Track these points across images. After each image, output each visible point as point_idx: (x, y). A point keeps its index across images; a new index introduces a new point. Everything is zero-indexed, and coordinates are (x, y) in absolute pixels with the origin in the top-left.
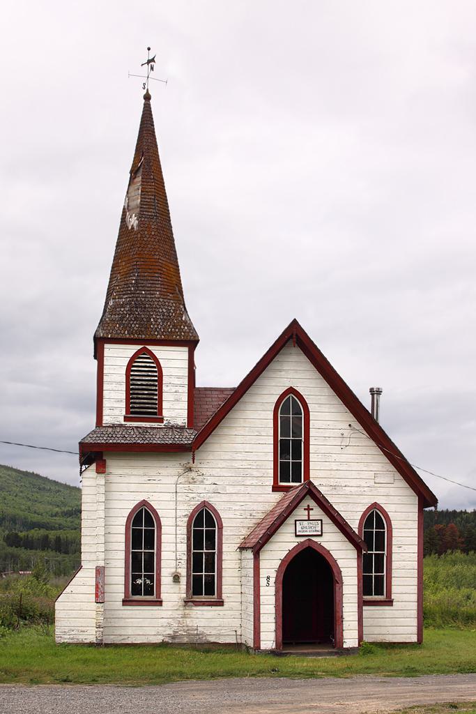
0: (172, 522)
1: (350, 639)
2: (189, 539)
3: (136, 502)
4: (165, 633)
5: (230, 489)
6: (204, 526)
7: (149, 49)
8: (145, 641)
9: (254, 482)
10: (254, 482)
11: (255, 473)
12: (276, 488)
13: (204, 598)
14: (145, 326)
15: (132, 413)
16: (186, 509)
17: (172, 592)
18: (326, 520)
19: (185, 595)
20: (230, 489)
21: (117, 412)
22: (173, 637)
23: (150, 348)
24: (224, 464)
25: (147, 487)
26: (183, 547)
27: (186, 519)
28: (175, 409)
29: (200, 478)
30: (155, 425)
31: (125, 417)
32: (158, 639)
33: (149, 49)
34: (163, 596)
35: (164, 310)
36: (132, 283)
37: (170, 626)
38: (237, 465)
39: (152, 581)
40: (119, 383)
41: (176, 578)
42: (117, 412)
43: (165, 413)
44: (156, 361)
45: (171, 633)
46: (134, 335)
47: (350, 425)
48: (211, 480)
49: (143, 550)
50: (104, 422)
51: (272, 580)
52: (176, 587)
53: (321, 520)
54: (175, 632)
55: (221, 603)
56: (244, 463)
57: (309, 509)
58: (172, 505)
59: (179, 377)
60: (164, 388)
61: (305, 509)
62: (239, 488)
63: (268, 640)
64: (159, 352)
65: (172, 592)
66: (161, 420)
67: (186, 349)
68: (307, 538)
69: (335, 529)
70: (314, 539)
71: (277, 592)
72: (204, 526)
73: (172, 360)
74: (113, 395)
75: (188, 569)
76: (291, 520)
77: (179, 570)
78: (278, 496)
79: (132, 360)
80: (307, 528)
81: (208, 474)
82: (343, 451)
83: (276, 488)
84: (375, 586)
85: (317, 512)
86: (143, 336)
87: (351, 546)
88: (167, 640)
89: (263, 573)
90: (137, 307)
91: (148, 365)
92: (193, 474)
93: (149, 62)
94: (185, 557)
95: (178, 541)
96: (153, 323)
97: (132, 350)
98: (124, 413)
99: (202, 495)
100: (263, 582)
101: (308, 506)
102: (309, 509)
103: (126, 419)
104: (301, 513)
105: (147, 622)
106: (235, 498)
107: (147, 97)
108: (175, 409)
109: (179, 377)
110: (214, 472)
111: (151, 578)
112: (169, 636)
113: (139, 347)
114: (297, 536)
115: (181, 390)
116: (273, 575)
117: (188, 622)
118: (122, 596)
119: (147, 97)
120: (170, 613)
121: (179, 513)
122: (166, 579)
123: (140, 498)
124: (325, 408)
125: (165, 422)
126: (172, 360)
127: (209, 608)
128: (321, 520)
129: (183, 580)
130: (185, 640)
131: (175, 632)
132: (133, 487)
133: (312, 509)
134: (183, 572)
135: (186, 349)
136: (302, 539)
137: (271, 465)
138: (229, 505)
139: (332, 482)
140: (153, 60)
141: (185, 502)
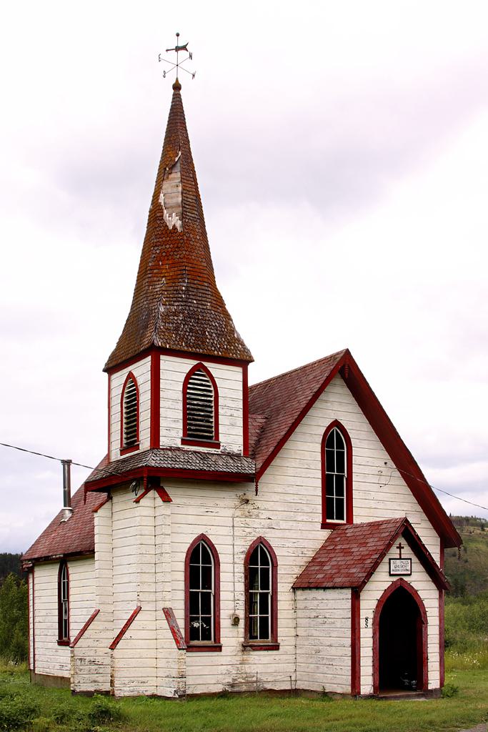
0: (230, 559)
1: (433, 682)
3: (195, 536)
4: (224, 682)
5: (283, 525)
6: (259, 562)
7: (178, 35)
8: (206, 691)
9: (305, 518)
11: (306, 509)
12: (325, 526)
13: (259, 642)
14: (201, 338)
16: (243, 546)
17: (231, 636)
19: (243, 640)
20: (283, 525)
21: (173, 433)
22: (232, 686)
23: (206, 364)
24: (276, 497)
25: (205, 520)
28: (231, 435)
29: (256, 512)
30: (213, 451)
31: (182, 440)
32: (218, 688)
33: (178, 35)
34: (223, 641)
35: (217, 325)
36: (182, 290)
37: (229, 673)
38: (289, 498)
40: (175, 400)
41: (236, 621)
42: (173, 433)
43: (222, 439)
45: (231, 681)
46: (191, 348)
47: (386, 463)
48: (265, 514)
49: (200, 590)
51: (370, 621)
52: (235, 629)
53: (411, 559)
54: (234, 680)
55: (276, 647)
56: (295, 497)
57: (400, 547)
59: (233, 400)
61: (397, 548)
62: (291, 523)
63: (367, 686)
64: (216, 369)
65: (231, 636)
66: (217, 446)
67: (240, 369)
68: (398, 578)
71: (374, 633)
72: (259, 562)
73: (227, 379)
76: (386, 560)
77: (237, 612)
78: (326, 534)
79: (188, 377)
80: (399, 567)
81: (263, 508)
82: (381, 489)
83: (325, 526)
85: (407, 551)
86: (201, 351)
90: (190, 318)
91: (204, 383)
92: (249, 507)
93: (178, 49)
95: (236, 580)
96: (209, 337)
97: (188, 364)
98: (181, 434)
99: (257, 530)
100: (363, 622)
101: (400, 544)
102: (400, 547)
103: (184, 442)
104: (394, 552)
105: (207, 670)
106: (287, 534)
107: (177, 87)
108: (231, 435)
109: (233, 400)
110: (267, 505)
111: (207, 621)
114: (391, 575)
115: (236, 413)
116: (371, 616)
117: (247, 669)
119: (177, 87)
120: (229, 658)
121: (238, 549)
122: (225, 623)
124: (365, 444)
125: (221, 448)
126: (227, 379)
127: (265, 652)
128: (411, 559)
129: (242, 623)
130: (244, 688)
131: (234, 680)
132: (191, 519)
133: (403, 548)
135: (240, 369)
136: (395, 579)
140: (184, 48)
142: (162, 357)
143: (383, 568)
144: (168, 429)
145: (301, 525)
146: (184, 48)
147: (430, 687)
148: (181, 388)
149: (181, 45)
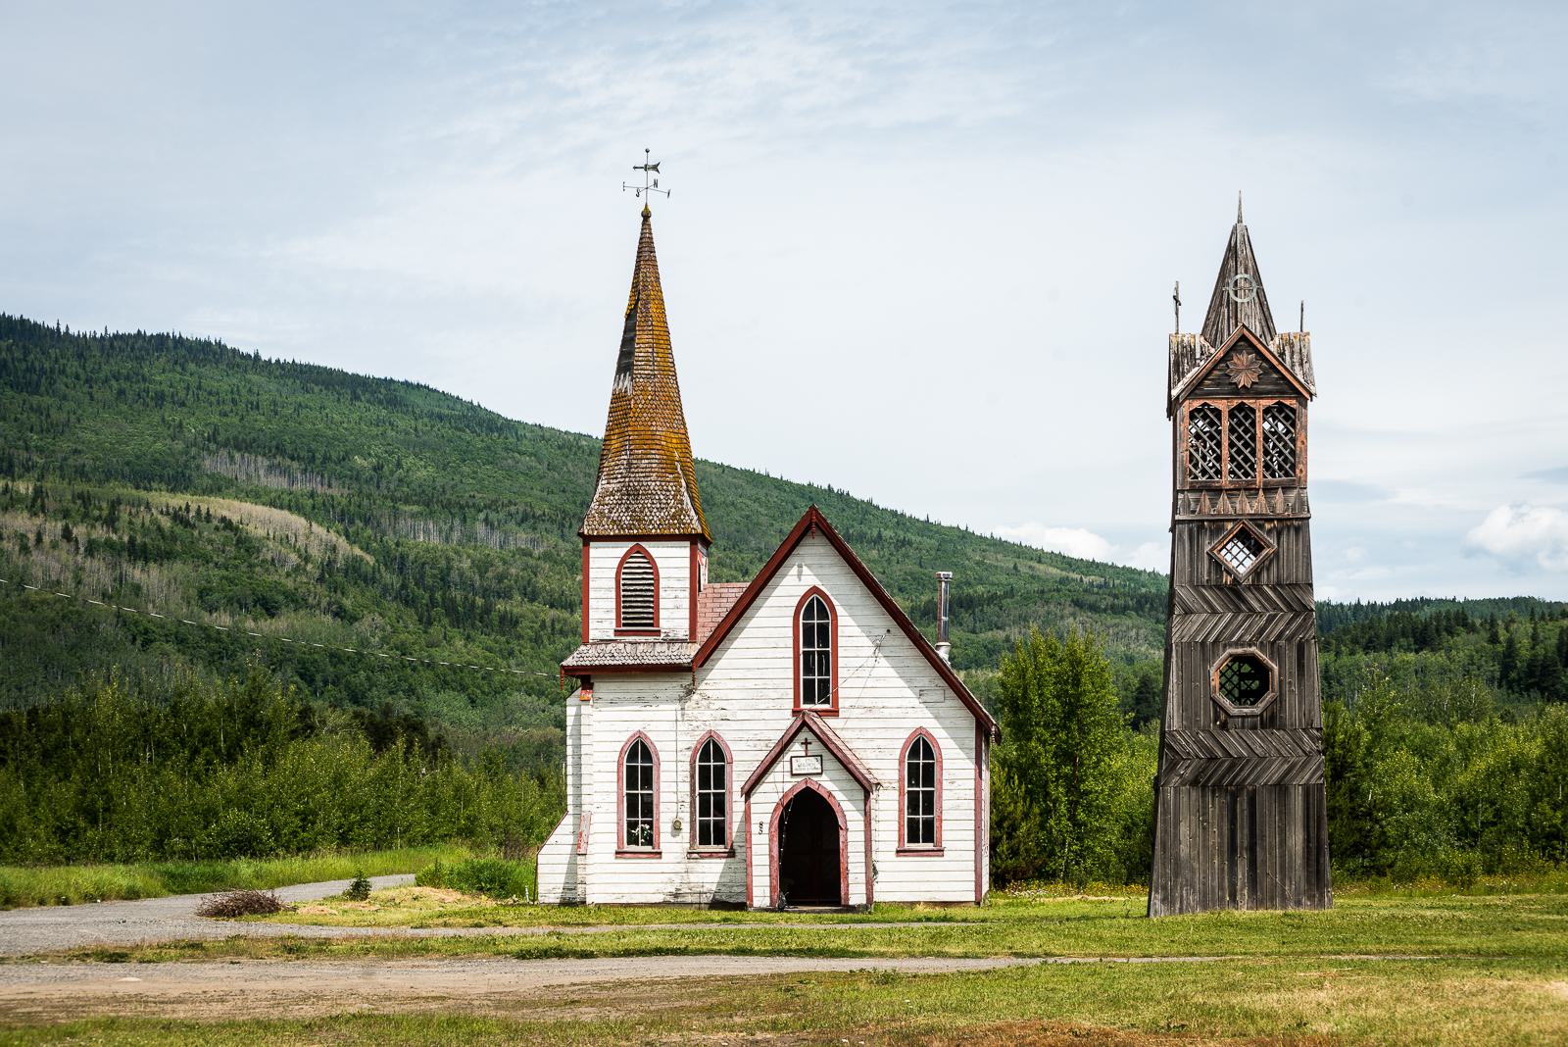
1: (856, 895)
2: (692, 776)
3: (630, 734)
6: (711, 761)
7: (647, 151)
8: (644, 901)
10: (771, 704)
13: (712, 848)
15: (624, 625)
16: (692, 739)
17: (674, 844)
18: (827, 755)
22: (676, 896)
23: (644, 544)
26: (687, 787)
27: (690, 753)
28: (673, 616)
29: (705, 703)
30: (651, 639)
32: (659, 898)
33: (647, 151)
34: (663, 848)
39: (651, 828)
40: (609, 589)
44: (651, 560)
45: (674, 891)
48: (718, 704)
49: (640, 792)
50: (591, 637)
54: (677, 889)
58: (672, 736)
59: (679, 579)
60: (662, 593)
63: (762, 892)
64: (655, 550)
65: (674, 844)
67: (688, 544)
69: (838, 765)
70: (815, 778)
72: (711, 761)
74: (602, 604)
75: (692, 813)
79: (623, 560)
84: (921, 830)
87: (856, 786)
88: (669, 898)
89: (755, 819)
90: (629, 495)
93: (646, 168)
94: (688, 799)
97: (620, 550)
98: (614, 626)
100: (755, 829)
102: (806, 743)
103: (617, 632)
104: (797, 748)
106: (747, 725)
107: (646, 216)
110: (722, 694)
111: (650, 823)
112: (671, 894)
113: (631, 544)
114: (793, 775)
116: (767, 819)
117: (693, 878)
118: (615, 848)
119: (646, 216)
121: (682, 746)
123: (636, 727)
125: (663, 635)
129: (686, 827)
130: (689, 899)
131: (677, 889)
134: (686, 817)
135: (688, 544)
137: (791, 684)
138: (741, 735)
139: (867, 703)
140: (655, 168)
141: (686, 732)
142: (592, 544)
143: (782, 766)
144: (600, 621)
145: (766, 715)
146: (655, 168)
147: (851, 902)
148: (613, 573)
149: (651, 163)
